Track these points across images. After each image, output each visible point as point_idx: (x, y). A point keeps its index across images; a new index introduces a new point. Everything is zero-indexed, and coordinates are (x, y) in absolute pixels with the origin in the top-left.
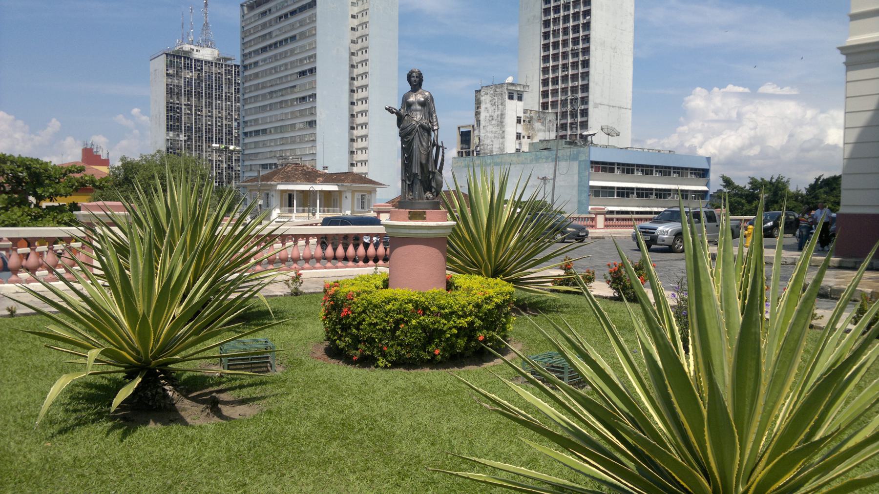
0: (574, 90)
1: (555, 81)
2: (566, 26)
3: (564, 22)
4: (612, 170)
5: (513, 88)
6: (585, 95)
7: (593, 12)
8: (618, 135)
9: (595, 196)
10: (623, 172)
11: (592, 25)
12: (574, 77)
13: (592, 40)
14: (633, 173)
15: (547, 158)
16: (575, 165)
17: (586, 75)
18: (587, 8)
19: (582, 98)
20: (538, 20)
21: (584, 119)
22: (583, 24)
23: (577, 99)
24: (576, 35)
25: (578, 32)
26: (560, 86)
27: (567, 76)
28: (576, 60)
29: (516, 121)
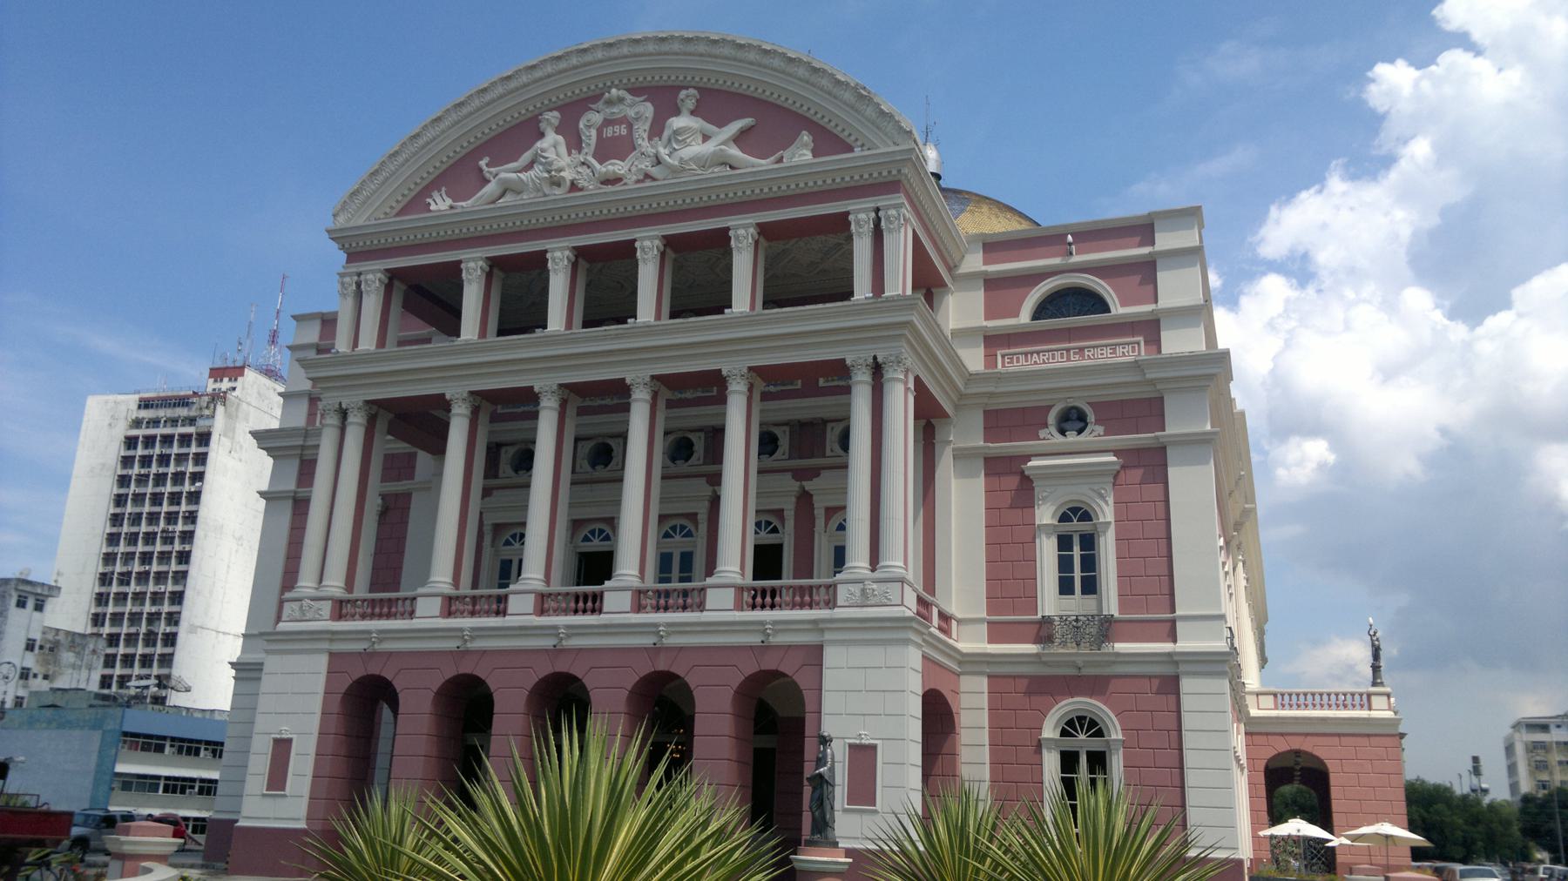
0: (157, 598)
1: (125, 579)
2: (158, 490)
3: (157, 484)
4: (160, 749)
5: (28, 588)
6: (175, 608)
7: (208, 477)
8: (188, 690)
9: (123, 789)
10: (180, 751)
11: (204, 497)
12: (161, 577)
13: (200, 520)
14: (197, 753)
15: (49, 722)
16: (97, 736)
17: (181, 577)
18: (199, 469)
19: (170, 614)
20: (111, 473)
21: (168, 650)
22: (190, 493)
23: (159, 614)
24: (174, 508)
25: (179, 504)
26: (133, 587)
27: (147, 573)
28: (167, 548)
29: (23, 646)
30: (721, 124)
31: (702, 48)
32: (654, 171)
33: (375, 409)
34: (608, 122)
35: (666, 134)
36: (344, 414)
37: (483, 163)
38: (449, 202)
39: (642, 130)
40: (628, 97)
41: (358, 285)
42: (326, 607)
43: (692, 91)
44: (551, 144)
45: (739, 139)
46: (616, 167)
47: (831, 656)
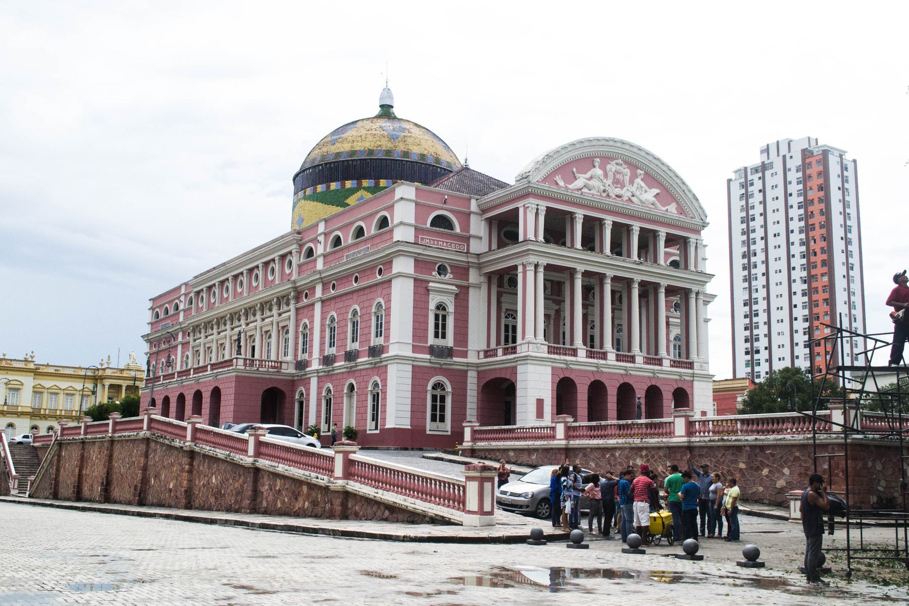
30: (650, 188)
31: (651, 158)
32: (634, 199)
33: (549, 268)
34: (617, 172)
35: (635, 185)
36: (536, 266)
37: (574, 170)
38: (562, 183)
39: (627, 178)
40: (624, 166)
41: (537, 209)
42: (546, 347)
43: (642, 172)
44: (598, 171)
45: (657, 196)
46: (618, 191)
47: (696, 384)
